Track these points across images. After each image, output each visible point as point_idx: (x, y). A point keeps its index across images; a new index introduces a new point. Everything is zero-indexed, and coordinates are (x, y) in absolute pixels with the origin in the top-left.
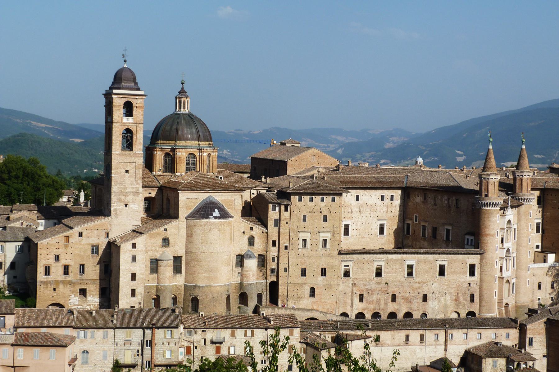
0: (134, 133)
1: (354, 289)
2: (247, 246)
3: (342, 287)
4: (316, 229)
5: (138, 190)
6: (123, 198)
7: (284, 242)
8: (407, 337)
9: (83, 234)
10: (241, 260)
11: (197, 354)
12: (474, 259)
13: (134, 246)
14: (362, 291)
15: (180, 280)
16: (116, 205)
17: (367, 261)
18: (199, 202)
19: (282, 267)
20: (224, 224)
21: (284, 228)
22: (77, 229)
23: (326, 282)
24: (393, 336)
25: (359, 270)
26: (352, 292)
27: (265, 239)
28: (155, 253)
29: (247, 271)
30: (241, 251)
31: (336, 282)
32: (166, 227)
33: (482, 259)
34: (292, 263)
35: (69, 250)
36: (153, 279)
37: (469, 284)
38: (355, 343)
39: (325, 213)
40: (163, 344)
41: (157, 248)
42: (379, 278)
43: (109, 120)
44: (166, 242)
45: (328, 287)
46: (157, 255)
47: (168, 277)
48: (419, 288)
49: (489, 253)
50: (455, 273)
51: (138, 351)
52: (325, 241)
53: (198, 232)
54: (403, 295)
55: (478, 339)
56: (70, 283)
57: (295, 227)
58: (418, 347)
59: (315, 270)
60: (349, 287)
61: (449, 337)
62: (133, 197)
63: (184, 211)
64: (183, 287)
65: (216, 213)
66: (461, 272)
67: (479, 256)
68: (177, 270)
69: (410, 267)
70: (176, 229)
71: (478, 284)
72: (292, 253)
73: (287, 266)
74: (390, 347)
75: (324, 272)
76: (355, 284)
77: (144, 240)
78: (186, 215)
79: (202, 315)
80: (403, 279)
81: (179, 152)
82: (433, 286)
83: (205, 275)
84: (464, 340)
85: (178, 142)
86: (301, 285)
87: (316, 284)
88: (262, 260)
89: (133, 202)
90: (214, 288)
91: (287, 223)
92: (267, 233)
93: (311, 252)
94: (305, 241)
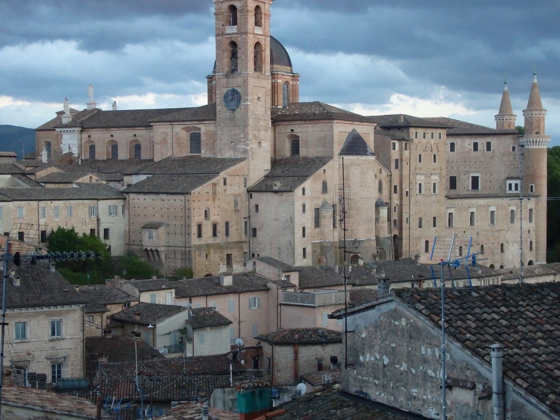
9: (228, 181)
16: (253, 145)
22: (223, 174)
27: (389, 184)
32: (325, 167)
33: (537, 203)
35: (217, 203)
42: (472, 227)
43: (231, 30)
56: (219, 247)
70: (331, 171)
80: (488, 228)
86: (419, 238)
89: (264, 140)
92: (391, 175)
94: (420, 185)
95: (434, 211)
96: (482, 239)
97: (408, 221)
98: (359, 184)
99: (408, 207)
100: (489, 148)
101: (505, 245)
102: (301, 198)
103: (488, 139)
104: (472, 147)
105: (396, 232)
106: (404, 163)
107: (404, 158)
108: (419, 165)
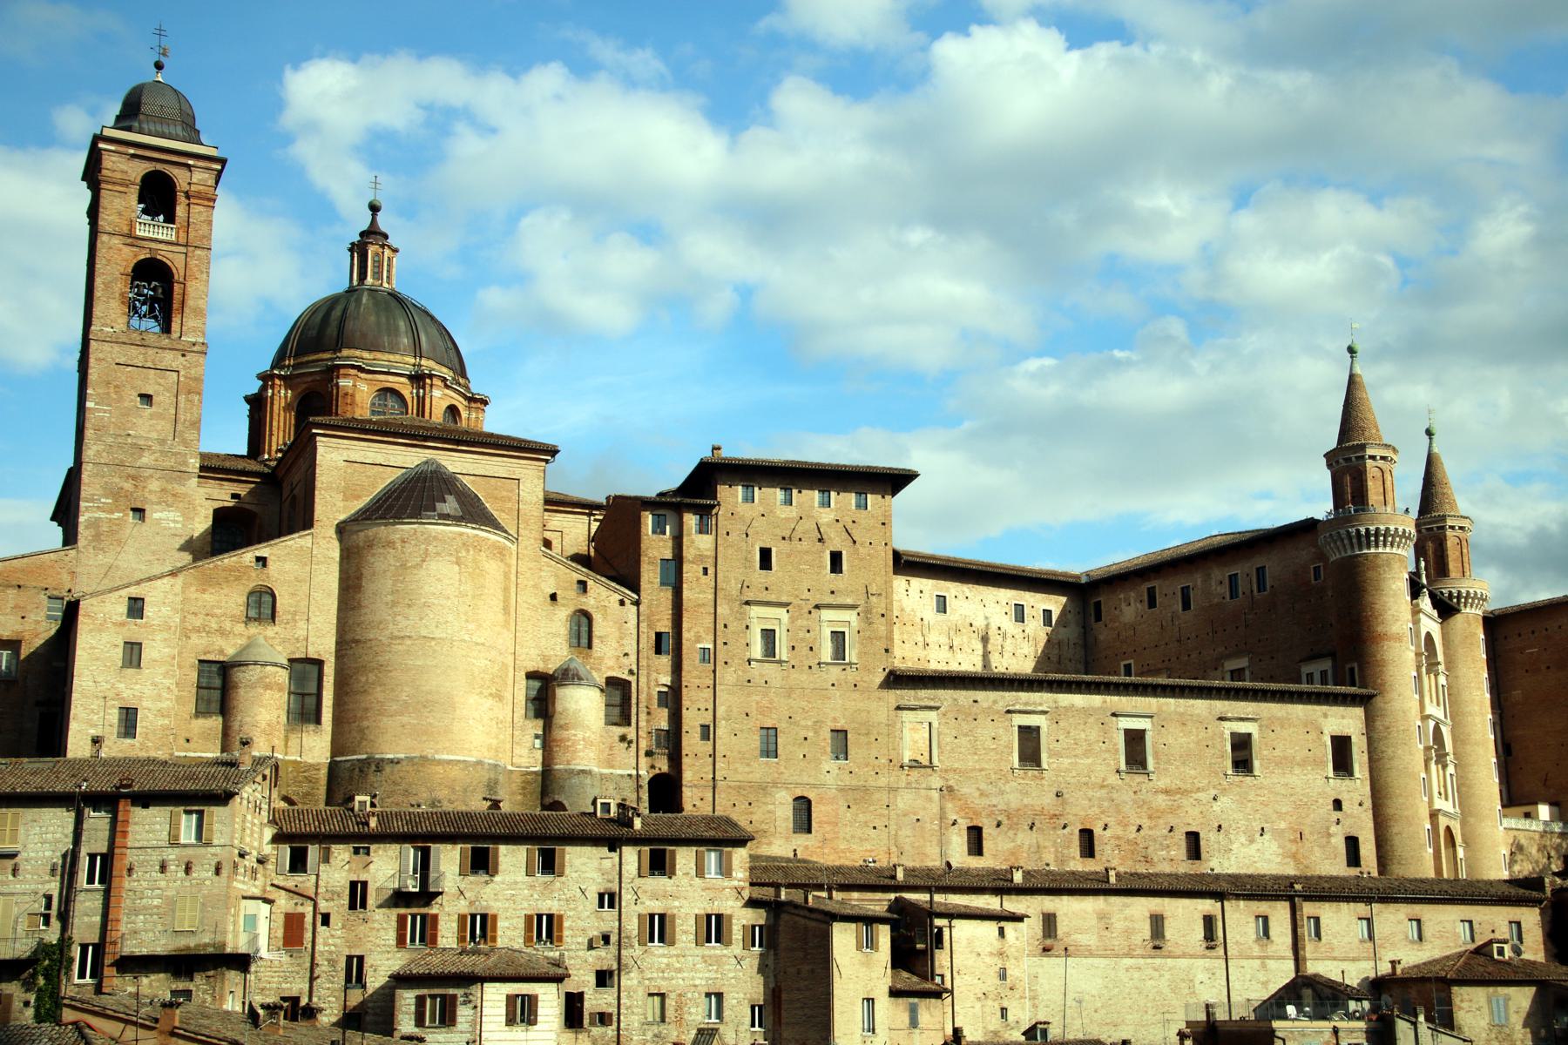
0: (178, 275)
1: (949, 805)
2: (565, 646)
3: (904, 801)
4: (806, 595)
5: (185, 463)
6: (128, 486)
7: (696, 636)
8: (1157, 922)
10: (544, 693)
11: (332, 943)
12: (1348, 721)
13: (136, 607)
14: (978, 814)
15: (316, 747)
17: (988, 711)
18: (389, 477)
19: (692, 720)
20: (478, 546)
21: (696, 591)
23: (848, 780)
24: (1102, 916)
25: (963, 741)
26: (942, 817)
28: (219, 642)
29: (564, 727)
30: (545, 659)
31: (883, 781)
32: (263, 550)
33: (1370, 721)
34: (728, 706)
36: (205, 736)
37: (1338, 804)
38: (962, 931)
39: (837, 542)
40: (163, 868)
41: (228, 625)
44: (263, 605)
45: (857, 795)
46: (228, 649)
47: (263, 725)
48: (1173, 810)
49: (1394, 695)
50: (1285, 763)
51: (49, 898)
52: (838, 637)
53: (381, 565)
54: (1120, 833)
55: (1412, 942)
57: (734, 587)
58: (1201, 962)
59: (810, 734)
60: (930, 799)
61: (1307, 929)
62: (163, 484)
63: (331, 506)
64: (324, 772)
65: (450, 505)
66: (1303, 763)
67: (1359, 712)
68: (305, 712)
69: (1135, 740)
70: (304, 566)
71: (1368, 803)
72: (727, 676)
73: (708, 720)
74: (1096, 961)
75: (841, 741)
76: (950, 789)
77: (178, 589)
78: (342, 517)
79: (363, 803)
81: (346, 376)
82: (1217, 806)
83: (405, 719)
84: (1362, 941)
85: (345, 352)
86: (763, 788)
87: (814, 786)
88: (619, 694)
90: (440, 769)
91: (705, 571)
92: (637, 603)
93: (794, 674)
94: (769, 636)
95: (837, 711)
96: (1081, 811)
97: (706, 732)
98: (390, 598)
99: (708, 693)
100: (1261, 586)
101: (1208, 840)
102: (122, 624)
103: (1259, 561)
104: (1225, 590)
105: (663, 765)
106: (690, 571)
107: (688, 553)
108: (759, 577)
